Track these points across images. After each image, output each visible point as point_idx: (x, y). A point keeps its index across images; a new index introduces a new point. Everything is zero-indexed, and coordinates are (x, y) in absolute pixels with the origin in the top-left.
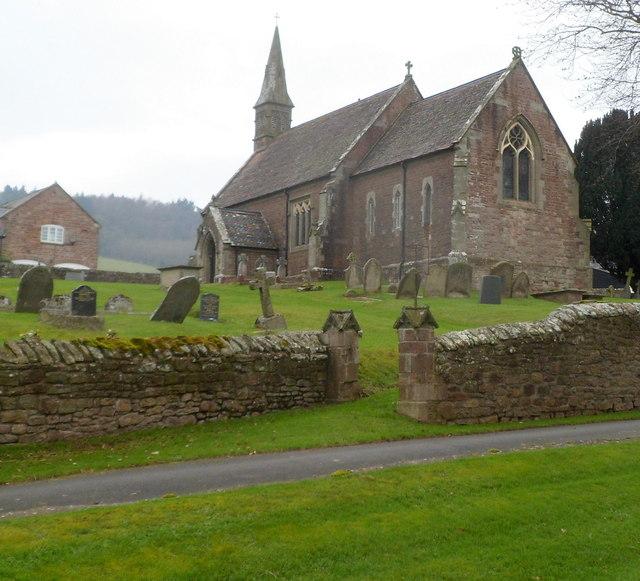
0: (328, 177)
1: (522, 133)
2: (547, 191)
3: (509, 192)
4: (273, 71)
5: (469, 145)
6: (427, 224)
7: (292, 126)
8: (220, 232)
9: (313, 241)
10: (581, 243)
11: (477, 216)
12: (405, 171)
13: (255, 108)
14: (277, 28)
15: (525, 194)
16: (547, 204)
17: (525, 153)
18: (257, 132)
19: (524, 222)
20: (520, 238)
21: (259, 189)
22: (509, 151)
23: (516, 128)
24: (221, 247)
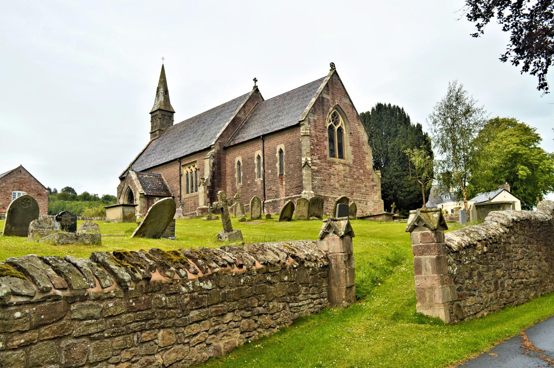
0: (209, 149)
1: (338, 116)
2: (354, 153)
3: (332, 155)
4: (162, 90)
5: (309, 123)
7: (174, 123)
8: (137, 186)
9: (201, 189)
10: (375, 186)
11: (316, 168)
12: (263, 142)
13: (151, 113)
15: (341, 156)
16: (354, 161)
17: (340, 129)
19: (343, 173)
20: (341, 182)
21: (159, 161)
22: (331, 127)
23: (335, 114)
24: (137, 196)
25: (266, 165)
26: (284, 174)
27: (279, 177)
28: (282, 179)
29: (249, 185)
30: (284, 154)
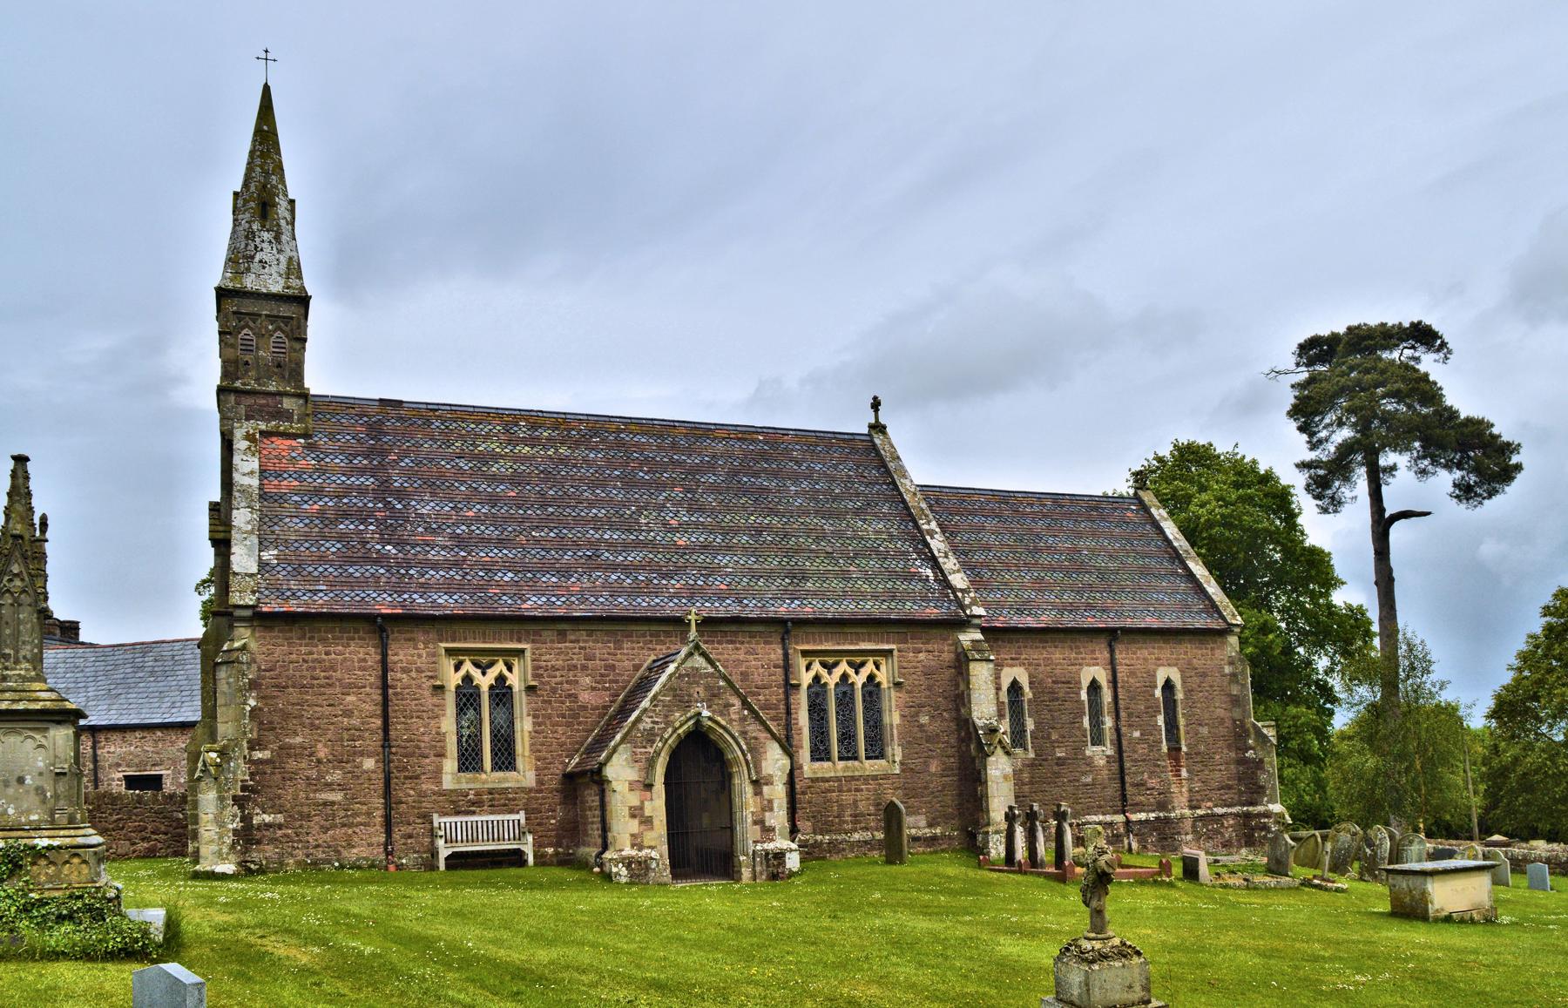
14: (266, 90)
18: (231, 369)
25: (1123, 714)
26: (1184, 749)
27: (1169, 755)
28: (1177, 760)
29: (1060, 762)
30: (1180, 696)
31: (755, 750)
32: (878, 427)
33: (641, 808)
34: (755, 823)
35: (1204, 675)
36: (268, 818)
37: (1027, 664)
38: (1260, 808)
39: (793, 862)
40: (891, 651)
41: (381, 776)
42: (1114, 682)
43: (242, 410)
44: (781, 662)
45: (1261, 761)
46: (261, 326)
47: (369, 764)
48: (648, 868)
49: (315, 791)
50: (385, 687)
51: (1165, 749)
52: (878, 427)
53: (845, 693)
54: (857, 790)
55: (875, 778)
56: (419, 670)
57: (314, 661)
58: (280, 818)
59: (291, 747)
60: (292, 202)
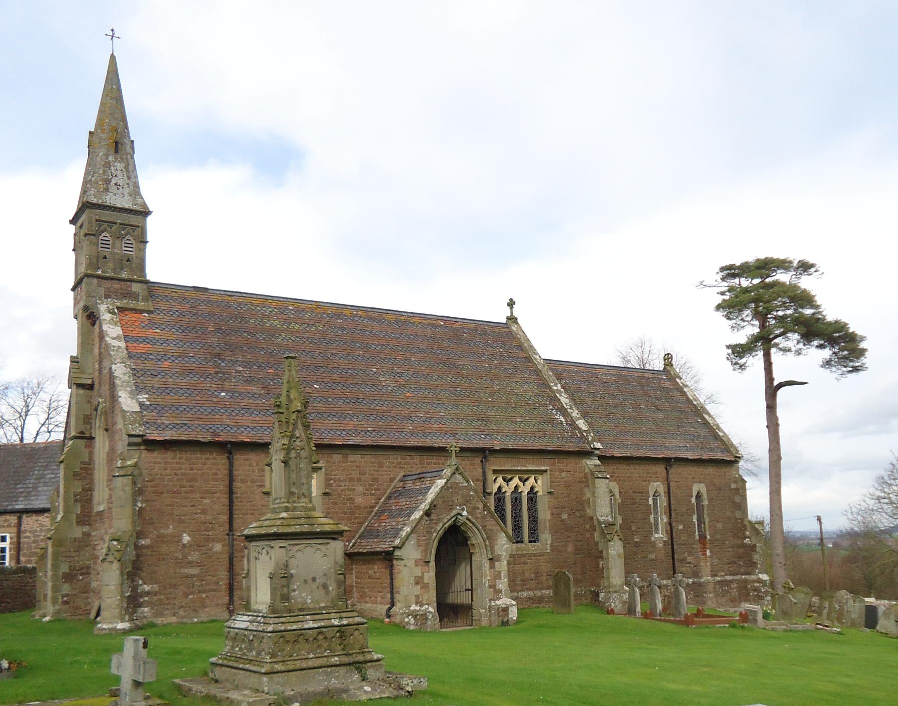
6: (703, 537)
14: (113, 58)
25: (673, 514)
26: (708, 537)
27: (699, 541)
28: (704, 544)
29: (637, 545)
30: (706, 503)
31: (490, 538)
32: (512, 319)
33: (422, 577)
34: (490, 587)
35: (720, 489)
36: (147, 588)
37: (619, 480)
38: (753, 577)
39: (513, 614)
40: (546, 471)
41: (227, 556)
42: (669, 493)
43: (102, 291)
44: (481, 478)
45: (755, 546)
46: (109, 228)
47: (218, 547)
48: (427, 619)
49: (180, 568)
50: (231, 492)
51: (697, 537)
52: (512, 319)
53: (516, 498)
54: (525, 563)
55: (535, 555)
56: (252, 481)
57: (182, 474)
58: (156, 587)
59: (164, 536)
60: (133, 142)
